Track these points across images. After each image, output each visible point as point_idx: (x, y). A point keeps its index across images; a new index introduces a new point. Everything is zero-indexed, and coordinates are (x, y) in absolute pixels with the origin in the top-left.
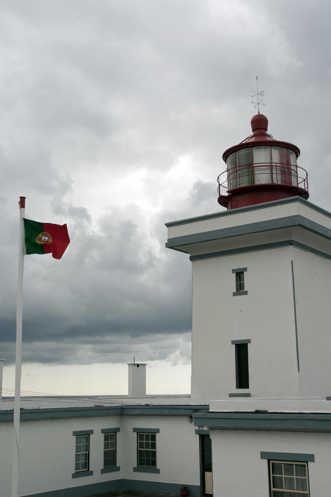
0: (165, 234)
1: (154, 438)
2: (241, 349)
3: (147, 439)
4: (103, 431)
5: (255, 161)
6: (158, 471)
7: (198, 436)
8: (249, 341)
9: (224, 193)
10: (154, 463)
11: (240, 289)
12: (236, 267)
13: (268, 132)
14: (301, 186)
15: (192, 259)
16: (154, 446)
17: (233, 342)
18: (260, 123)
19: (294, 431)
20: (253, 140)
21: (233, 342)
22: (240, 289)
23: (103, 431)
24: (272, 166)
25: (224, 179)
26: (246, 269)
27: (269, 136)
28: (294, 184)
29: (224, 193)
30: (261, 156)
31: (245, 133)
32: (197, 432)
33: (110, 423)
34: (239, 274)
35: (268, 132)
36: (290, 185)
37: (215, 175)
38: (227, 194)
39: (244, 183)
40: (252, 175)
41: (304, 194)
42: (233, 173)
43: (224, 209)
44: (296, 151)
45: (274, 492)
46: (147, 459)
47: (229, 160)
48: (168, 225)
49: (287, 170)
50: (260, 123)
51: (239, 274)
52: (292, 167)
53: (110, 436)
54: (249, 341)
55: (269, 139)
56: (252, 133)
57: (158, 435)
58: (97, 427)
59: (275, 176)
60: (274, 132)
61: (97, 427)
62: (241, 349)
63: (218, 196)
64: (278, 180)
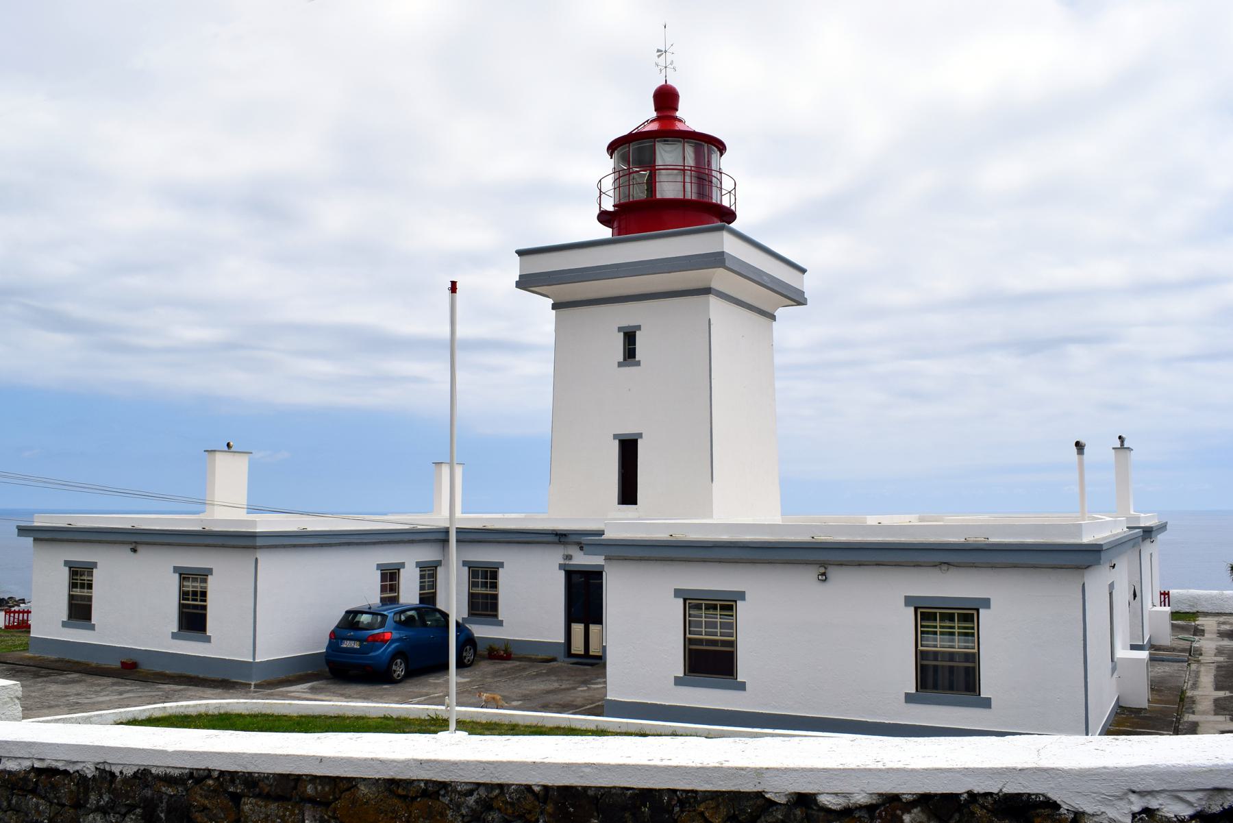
0: (514, 269)
1: (494, 575)
2: (628, 449)
3: (485, 576)
4: (418, 564)
5: (659, 162)
6: (500, 623)
7: (563, 573)
8: (640, 435)
9: (609, 206)
10: (495, 607)
11: (630, 353)
12: (625, 324)
13: (678, 114)
14: (726, 203)
15: (555, 306)
16: (494, 586)
17: (615, 436)
18: (666, 99)
19: (720, 561)
20: (654, 127)
21: (615, 436)
22: (630, 353)
23: (418, 564)
24: (684, 170)
25: (608, 184)
26: (639, 328)
27: (680, 121)
28: (715, 199)
29: (609, 206)
30: (666, 155)
31: (643, 114)
32: (561, 567)
33: (428, 554)
34: (630, 338)
35: (678, 114)
36: (706, 200)
37: (597, 178)
38: (611, 209)
39: (639, 194)
40: (651, 184)
41: (728, 215)
42: (622, 178)
43: (606, 232)
44: (721, 147)
45: (922, 652)
46: (484, 603)
47: (615, 154)
48: (521, 253)
49: (704, 177)
50: (666, 99)
51: (630, 338)
52: (714, 173)
53: (429, 572)
54: (640, 435)
55: (680, 126)
56: (654, 114)
57: (501, 572)
58: (410, 560)
59: (688, 186)
60: (691, 116)
61: (410, 560)
62: (628, 449)
63: (598, 212)
64: (691, 194)
